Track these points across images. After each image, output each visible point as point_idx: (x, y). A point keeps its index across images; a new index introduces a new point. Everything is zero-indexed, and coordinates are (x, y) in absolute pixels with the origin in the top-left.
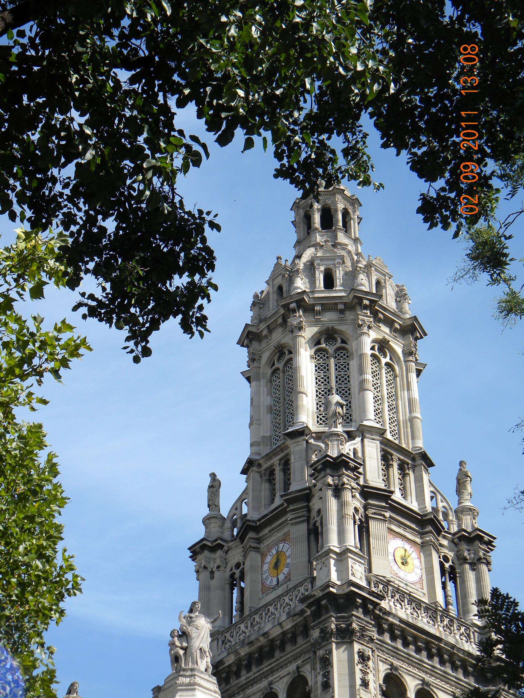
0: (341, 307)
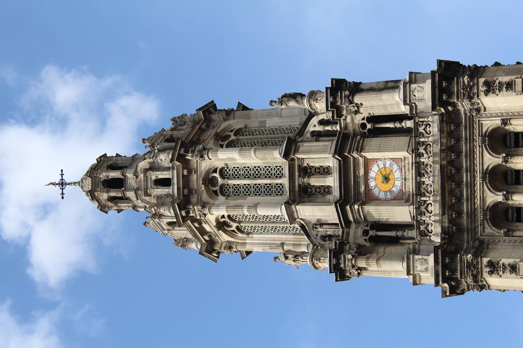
0: (196, 225)
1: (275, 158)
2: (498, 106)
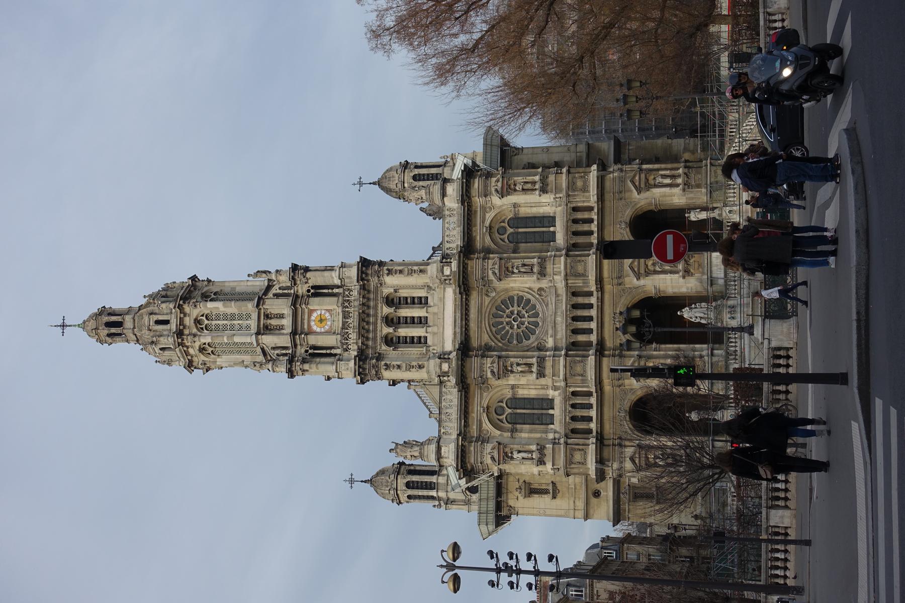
1: (250, 306)
2: (391, 282)
